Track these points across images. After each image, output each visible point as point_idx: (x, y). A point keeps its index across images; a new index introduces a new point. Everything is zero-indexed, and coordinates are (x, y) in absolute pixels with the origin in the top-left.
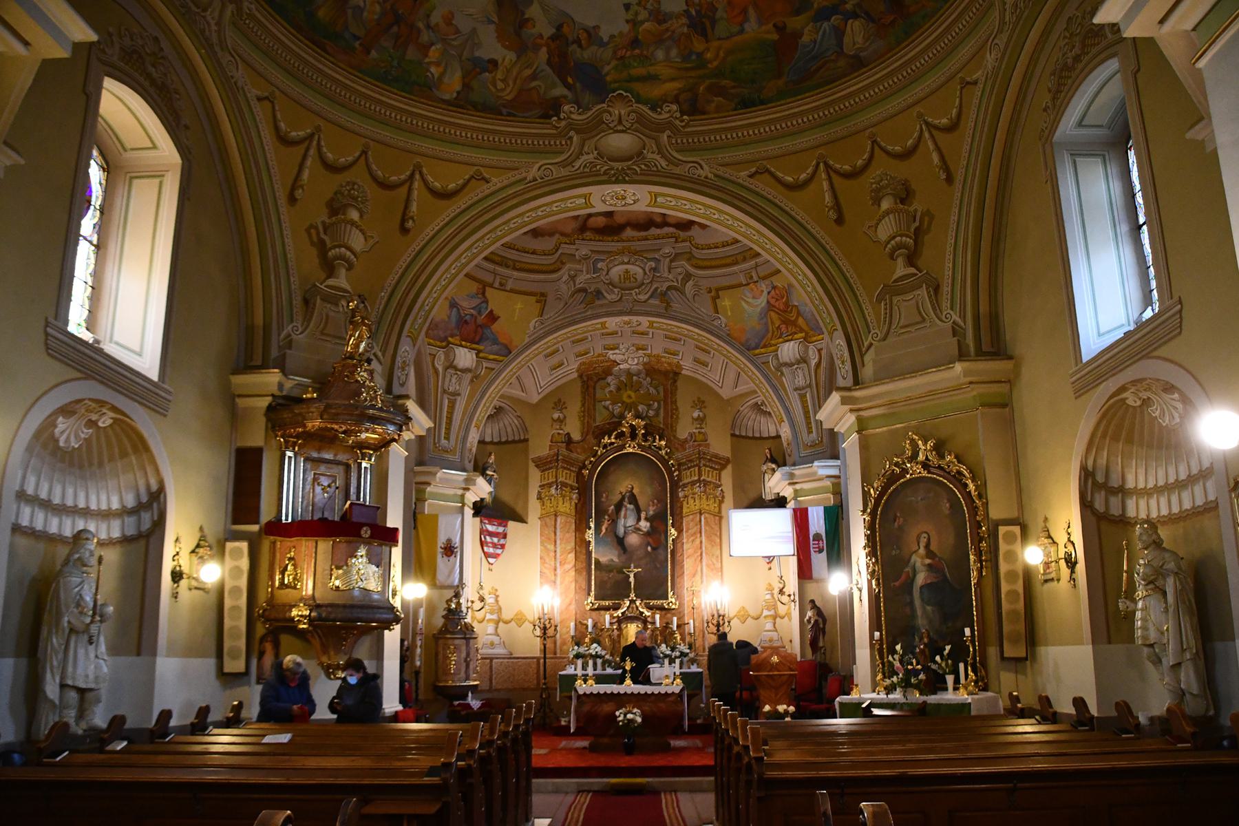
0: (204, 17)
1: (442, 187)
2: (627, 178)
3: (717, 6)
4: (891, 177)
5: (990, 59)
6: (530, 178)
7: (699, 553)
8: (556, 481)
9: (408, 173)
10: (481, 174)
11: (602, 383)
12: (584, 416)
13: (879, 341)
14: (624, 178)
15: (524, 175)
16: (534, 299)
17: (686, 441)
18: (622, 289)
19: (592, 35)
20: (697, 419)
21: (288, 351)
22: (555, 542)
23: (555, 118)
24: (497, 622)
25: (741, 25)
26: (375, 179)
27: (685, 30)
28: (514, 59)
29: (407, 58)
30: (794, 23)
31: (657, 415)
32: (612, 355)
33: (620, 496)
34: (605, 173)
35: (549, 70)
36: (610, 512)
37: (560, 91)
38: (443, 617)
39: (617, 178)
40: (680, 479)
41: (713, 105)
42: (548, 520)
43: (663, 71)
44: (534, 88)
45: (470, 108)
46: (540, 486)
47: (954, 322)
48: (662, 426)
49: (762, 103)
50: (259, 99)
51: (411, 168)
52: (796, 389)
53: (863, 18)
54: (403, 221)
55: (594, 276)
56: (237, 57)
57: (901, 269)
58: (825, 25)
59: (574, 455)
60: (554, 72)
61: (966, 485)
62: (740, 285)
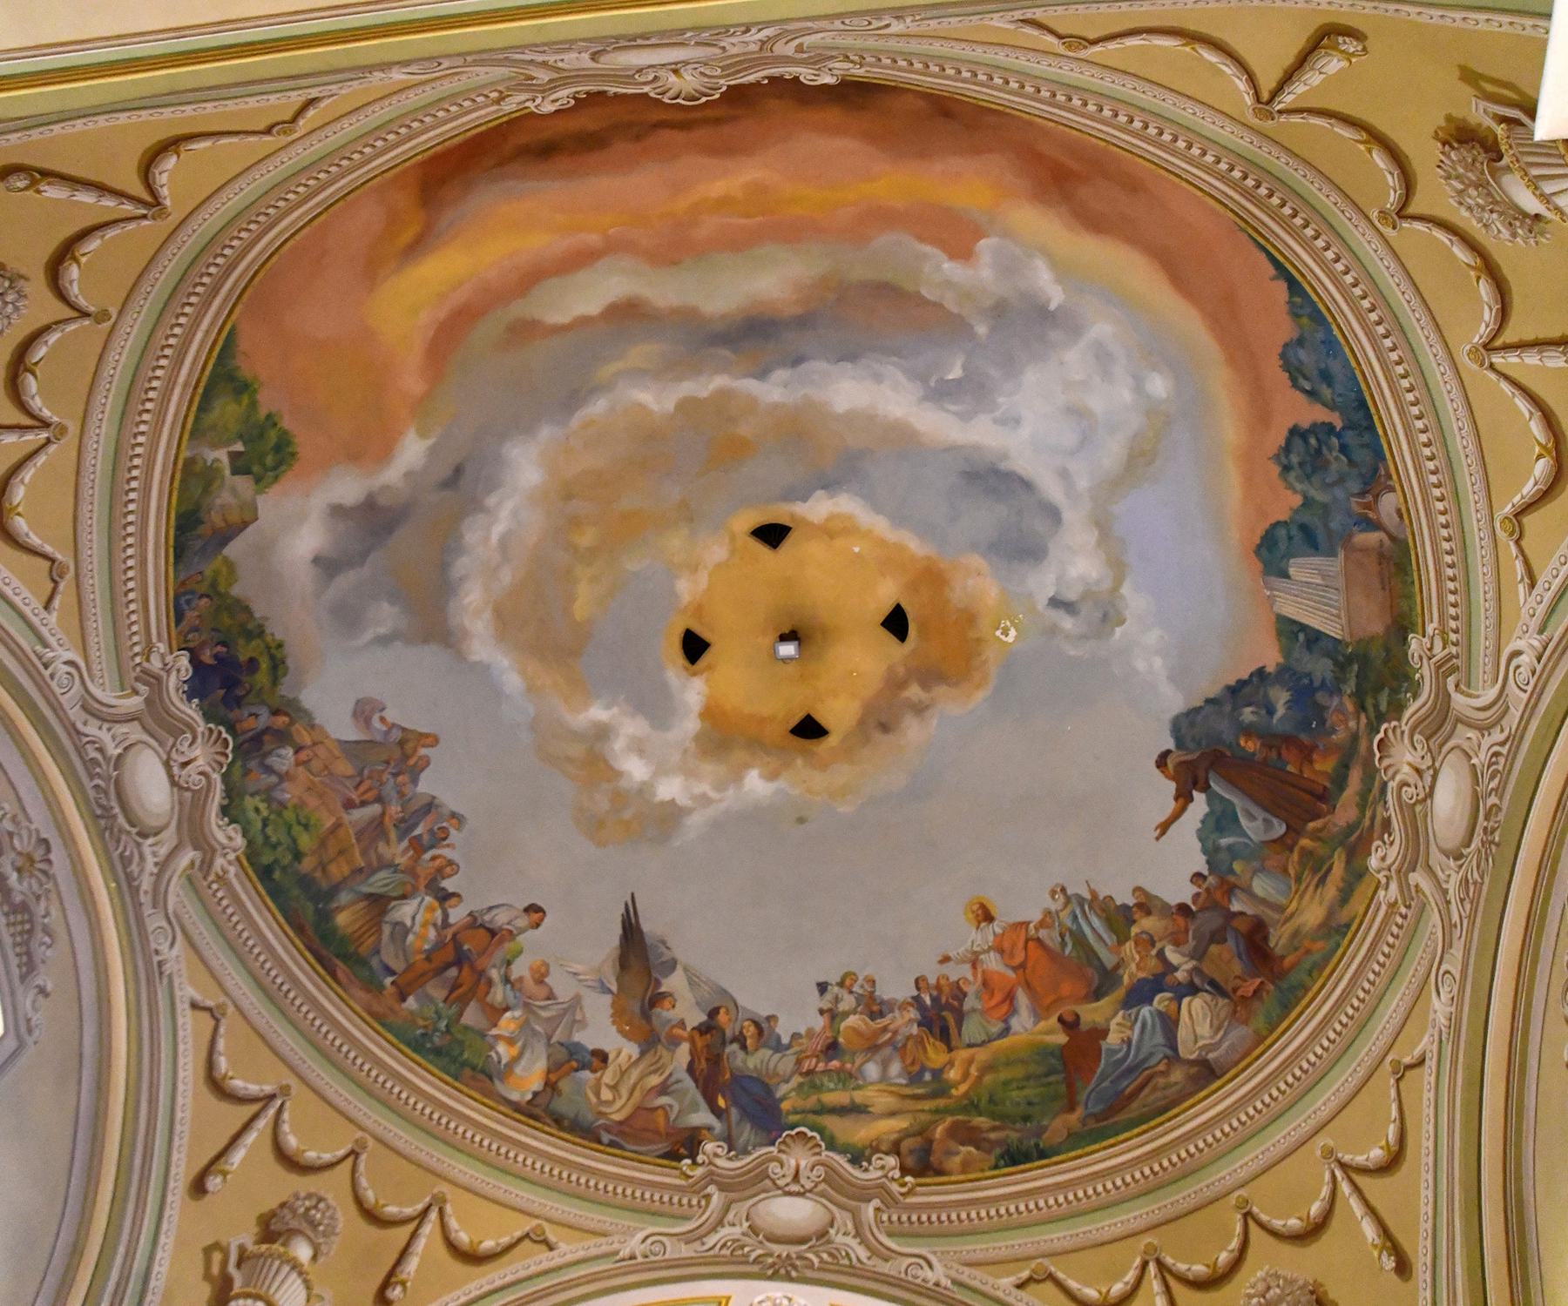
0: (139, 845)
1: (471, 1242)
2: (794, 1274)
3: (965, 988)
4: (1285, 1280)
5: (1440, 1007)
6: (625, 1253)
9: (420, 1207)
10: (544, 1233)
14: (788, 1273)
15: (616, 1246)
19: (763, 1029)
23: (688, 1161)
25: (1006, 1021)
26: (359, 1201)
27: (915, 1030)
28: (635, 1055)
29: (463, 1021)
30: (1092, 1013)
34: (756, 1261)
35: (689, 1082)
37: (702, 1117)
39: (776, 1273)
41: (957, 1160)
43: (882, 1101)
44: (662, 1107)
45: (549, 1121)
49: (1043, 1154)
50: (194, 1006)
51: (427, 1199)
53: (1207, 991)
56: (177, 929)
58: (1145, 1011)
60: (697, 1087)
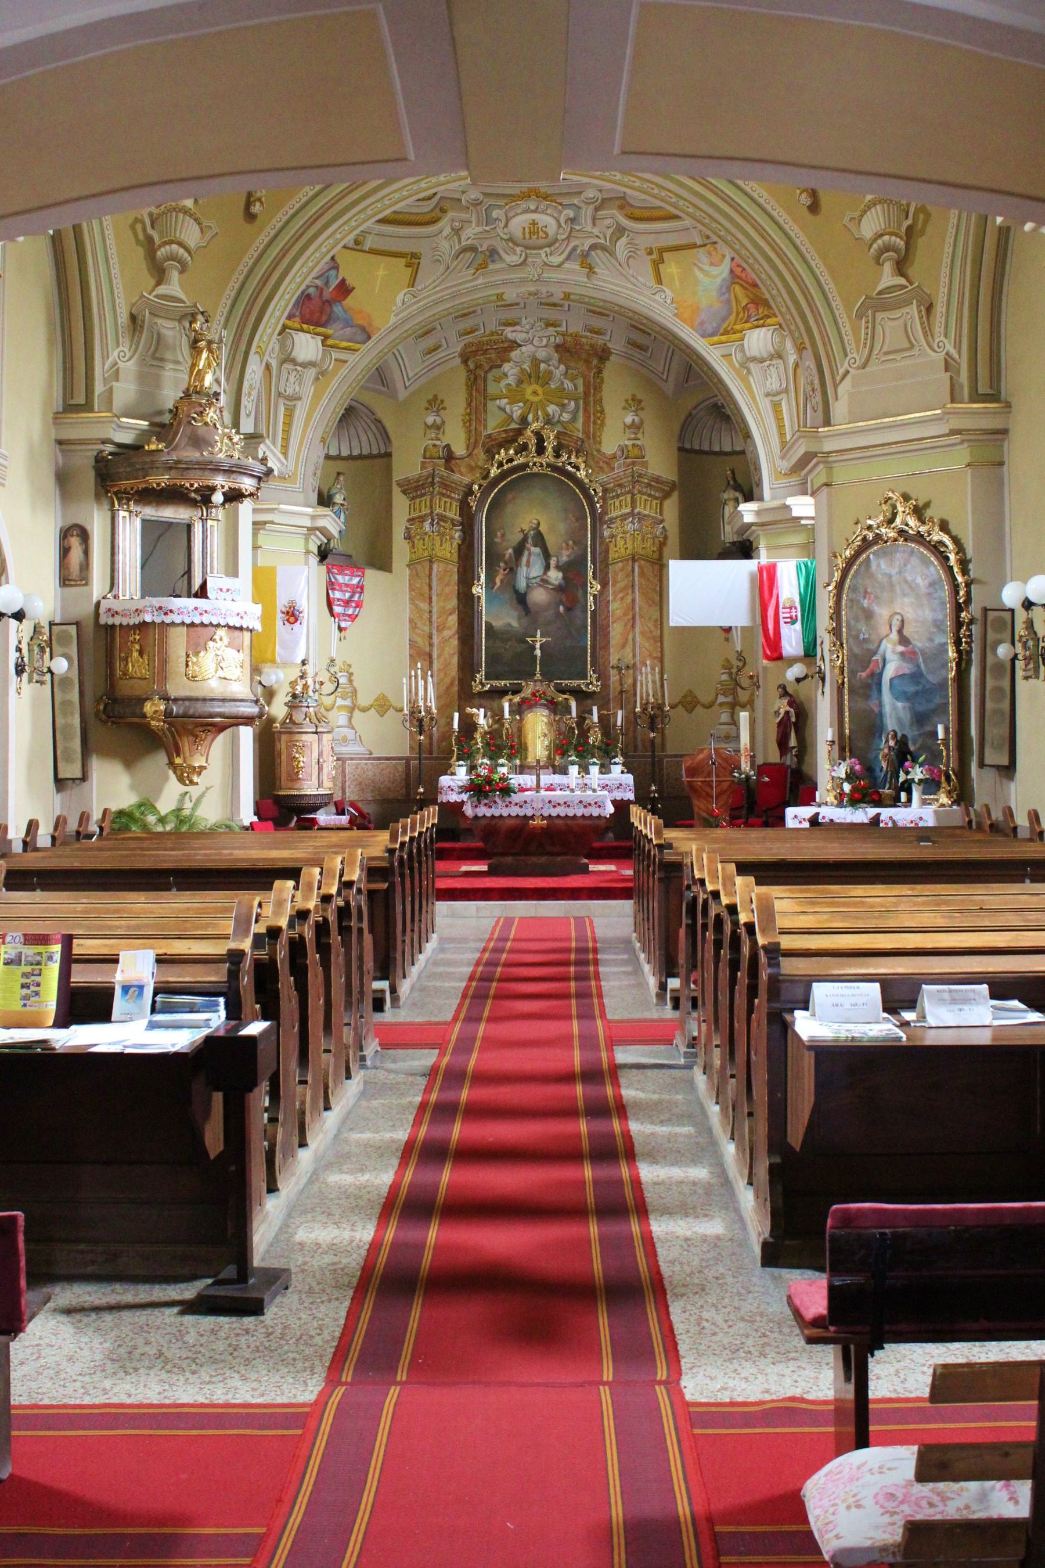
7: (630, 616)
8: (432, 512)
11: (495, 372)
12: (470, 420)
13: (858, 368)
16: (404, 260)
17: (614, 457)
18: (527, 248)
20: (630, 427)
21: (115, 384)
22: (430, 598)
24: (351, 710)
31: (574, 419)
32: (509, 333)
33: (521, 536)
36: (507, 556)
38: (286, 704)
40: (605, 512)
42: (419, 567)
46: (409, 520)
47: (947, 354)
48: (580, 436)
52: (768, 395)
54: (248, 204)
55: (487, 228)
57: (888, 278)
59: (456, 477)
61: (947, 559)
62: (694, 246)
